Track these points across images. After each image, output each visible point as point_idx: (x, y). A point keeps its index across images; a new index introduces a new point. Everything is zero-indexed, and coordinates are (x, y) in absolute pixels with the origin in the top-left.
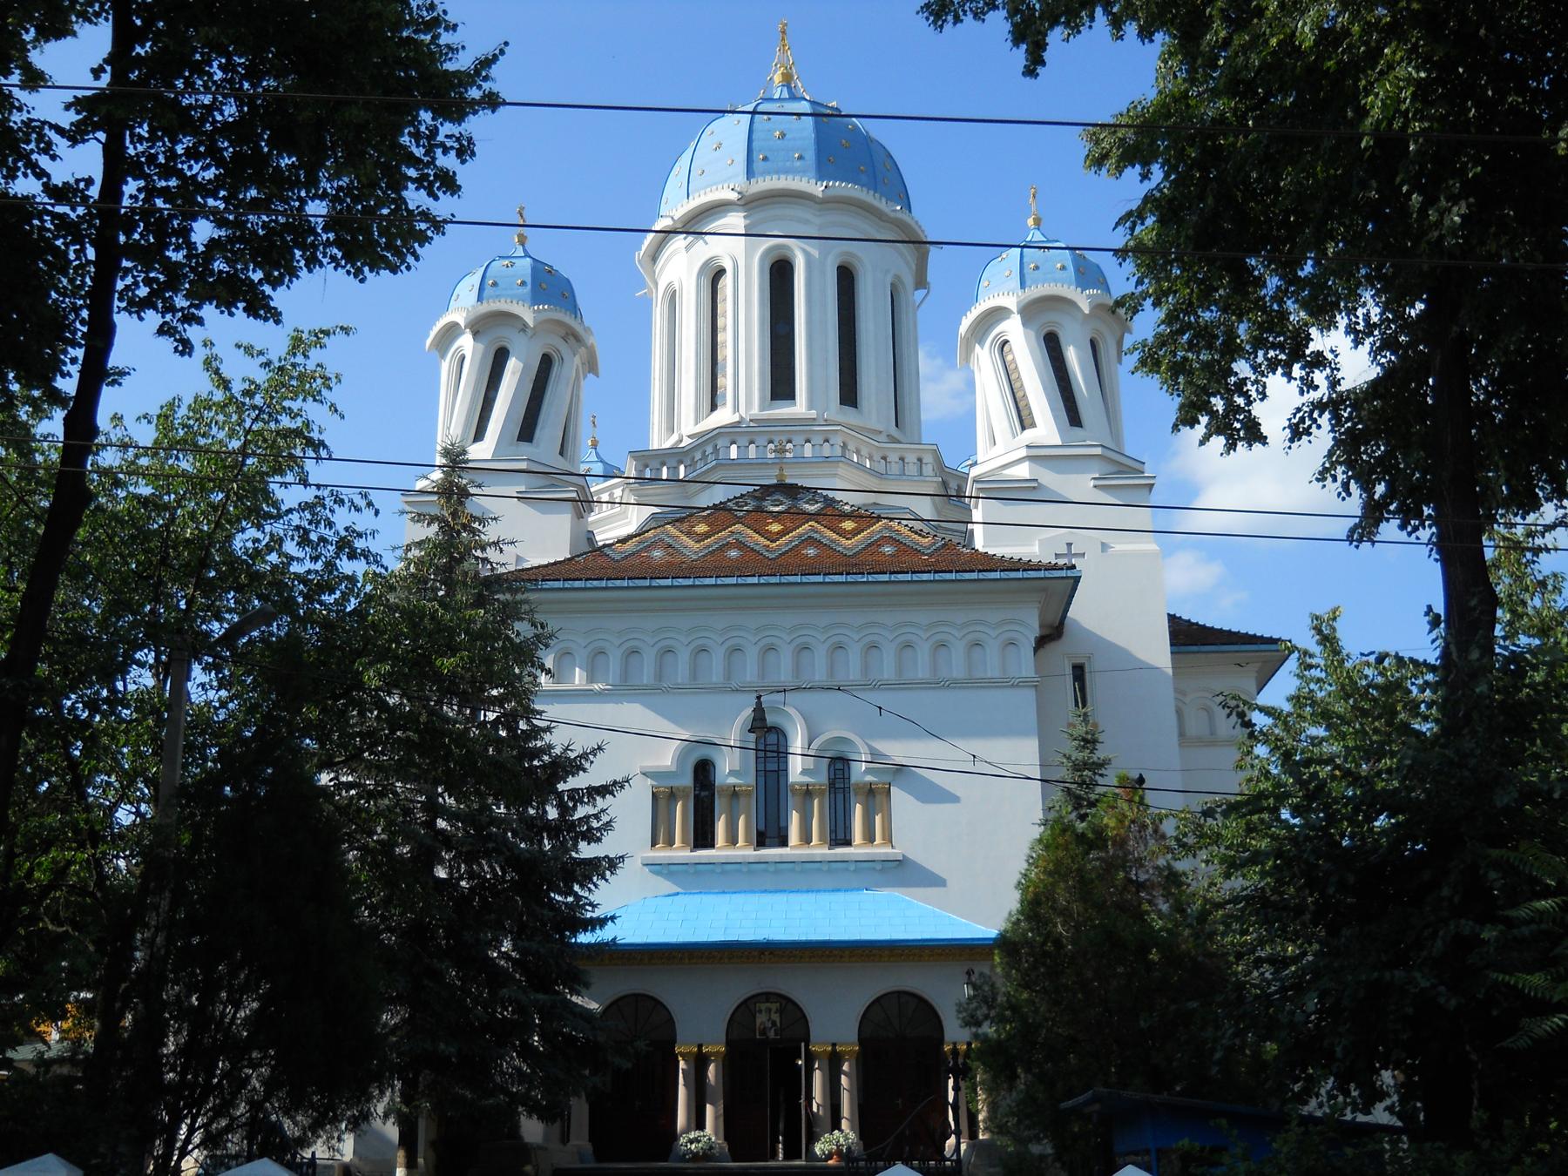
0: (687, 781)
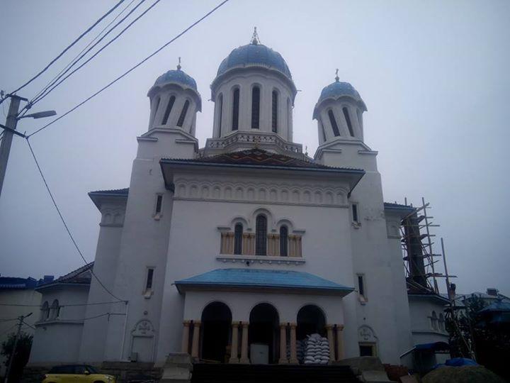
0: (233, 230)
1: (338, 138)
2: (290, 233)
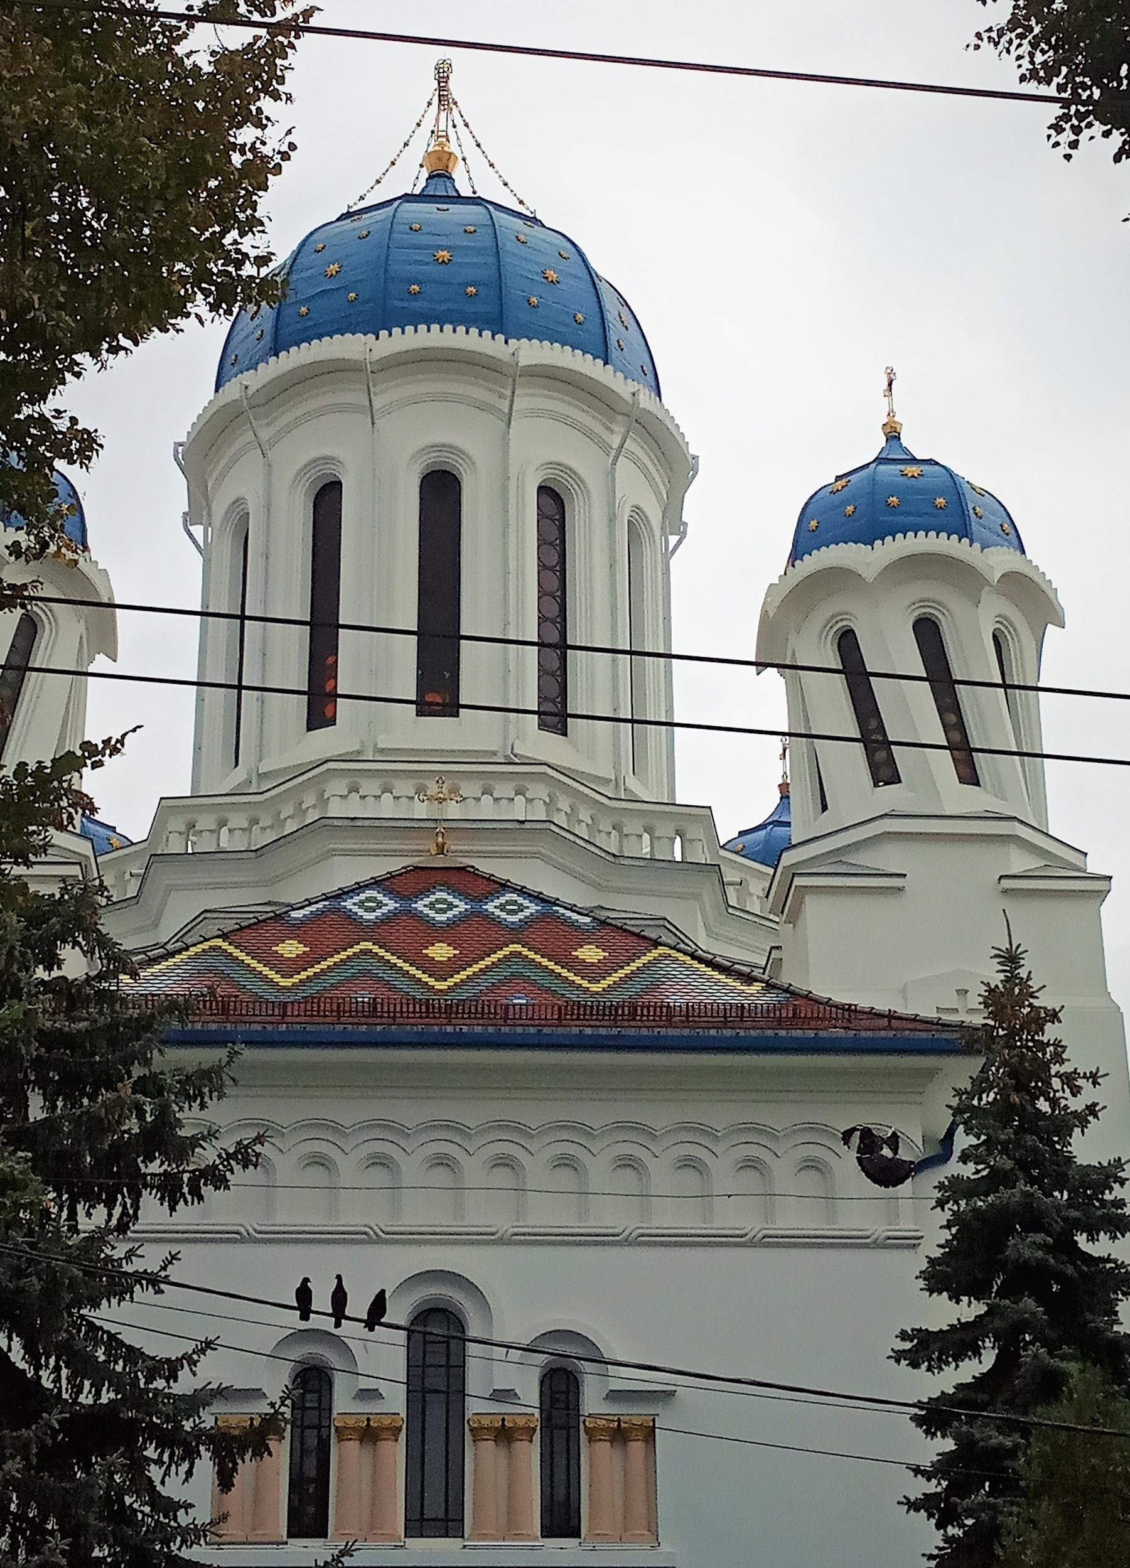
1: (889, 796)
2: (593, 1401)
